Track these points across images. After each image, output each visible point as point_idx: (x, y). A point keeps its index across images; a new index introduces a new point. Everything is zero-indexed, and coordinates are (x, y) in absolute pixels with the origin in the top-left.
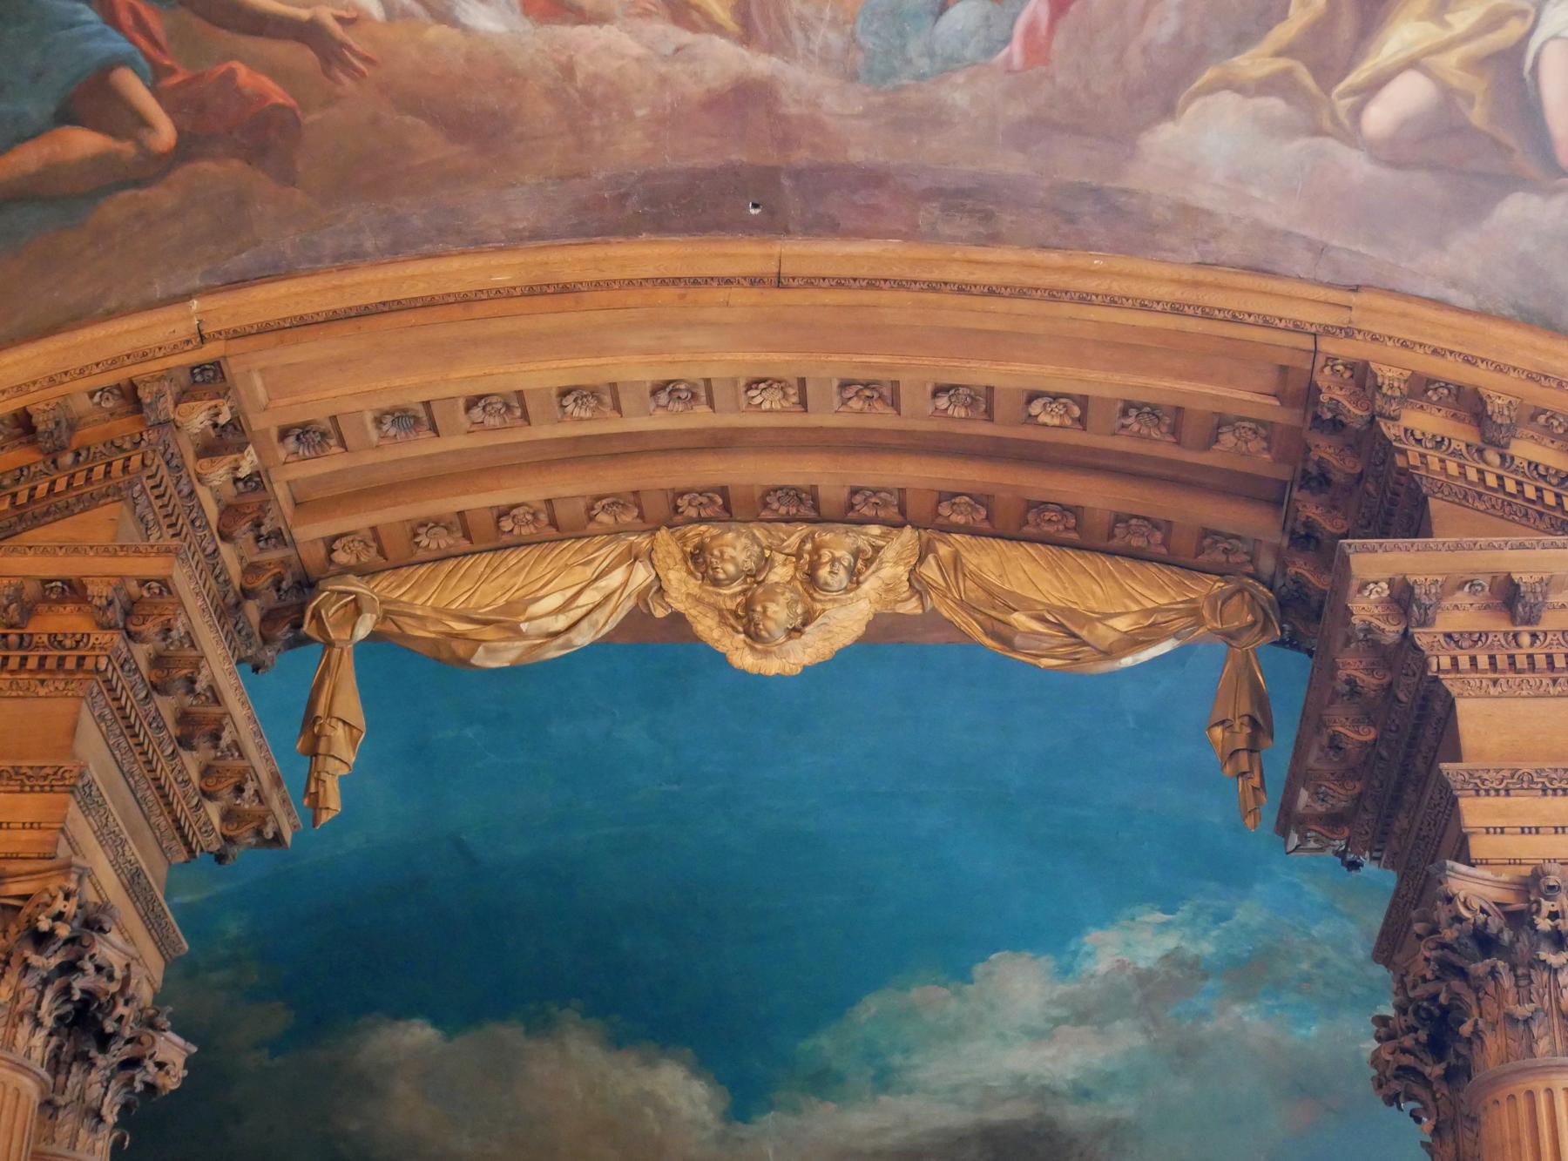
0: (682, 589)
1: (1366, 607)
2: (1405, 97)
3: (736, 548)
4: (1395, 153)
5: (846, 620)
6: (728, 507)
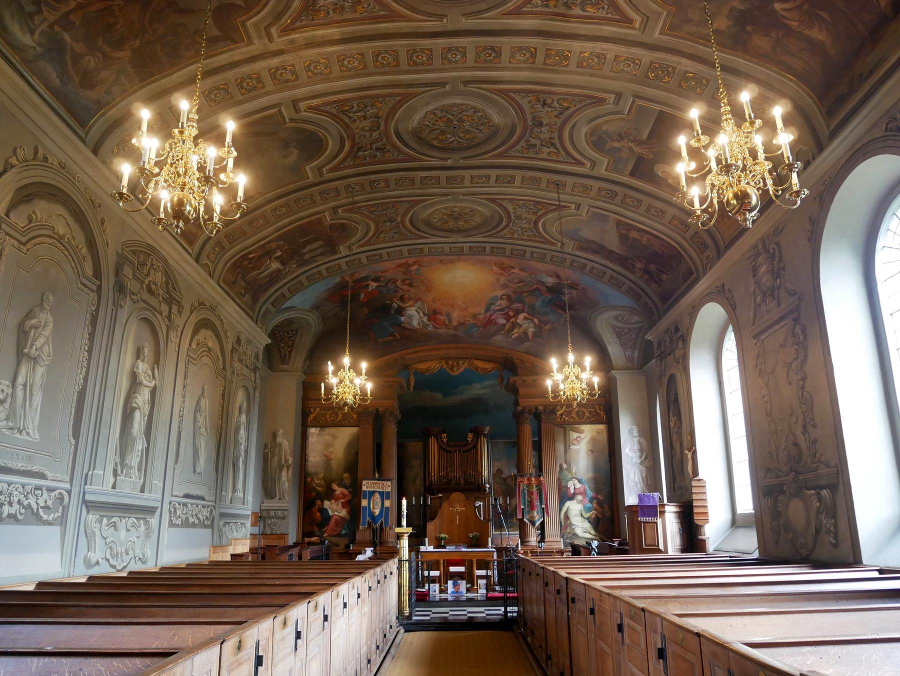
0: (445, 365)
1: (511, 381)
2: (516, 335)
3: (450, 362)
4: (516, 339)
5: (462, 369)
6: (450, 358)
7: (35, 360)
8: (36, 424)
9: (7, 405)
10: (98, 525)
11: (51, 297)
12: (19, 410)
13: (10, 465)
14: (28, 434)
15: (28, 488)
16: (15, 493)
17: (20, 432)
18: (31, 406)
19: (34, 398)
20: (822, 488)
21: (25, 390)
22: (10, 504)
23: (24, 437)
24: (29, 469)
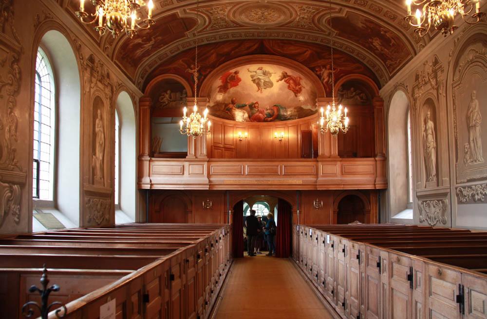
7: (475, 126)
8: (481, 155)
9: (469, 153)
10: (422, 205)
11: (475, 92)
12: (473, 152)
13: (474, 177)
14: (479, 161)
15: (484, 186)
16: (479, 189)
17: (476, 161)
18: (477, 147)
19: (478, 143)
20: (14, 183)
21: (474, 142)
22: (478, 194)
23: (478, 162)
24: (482, 176)
